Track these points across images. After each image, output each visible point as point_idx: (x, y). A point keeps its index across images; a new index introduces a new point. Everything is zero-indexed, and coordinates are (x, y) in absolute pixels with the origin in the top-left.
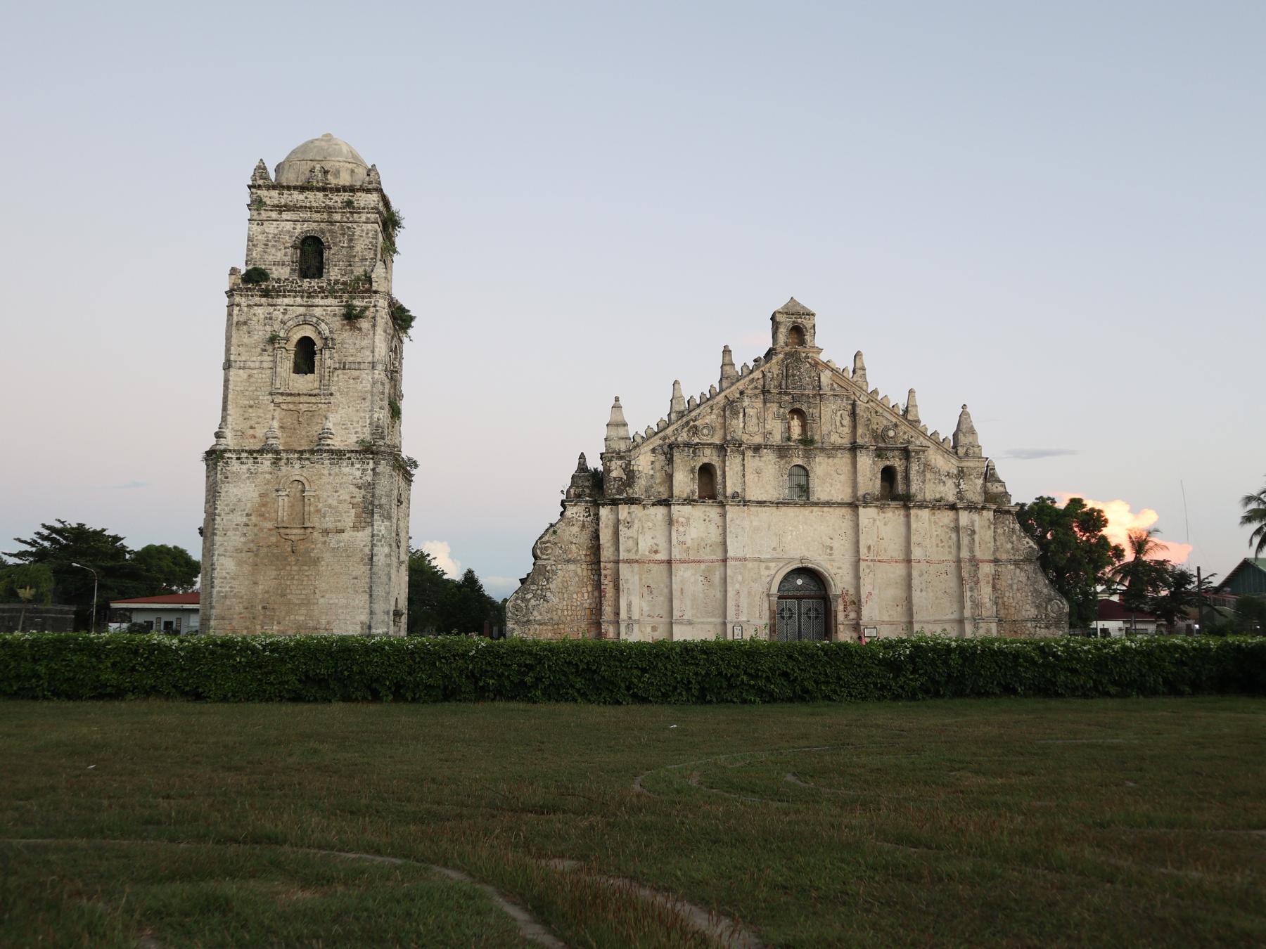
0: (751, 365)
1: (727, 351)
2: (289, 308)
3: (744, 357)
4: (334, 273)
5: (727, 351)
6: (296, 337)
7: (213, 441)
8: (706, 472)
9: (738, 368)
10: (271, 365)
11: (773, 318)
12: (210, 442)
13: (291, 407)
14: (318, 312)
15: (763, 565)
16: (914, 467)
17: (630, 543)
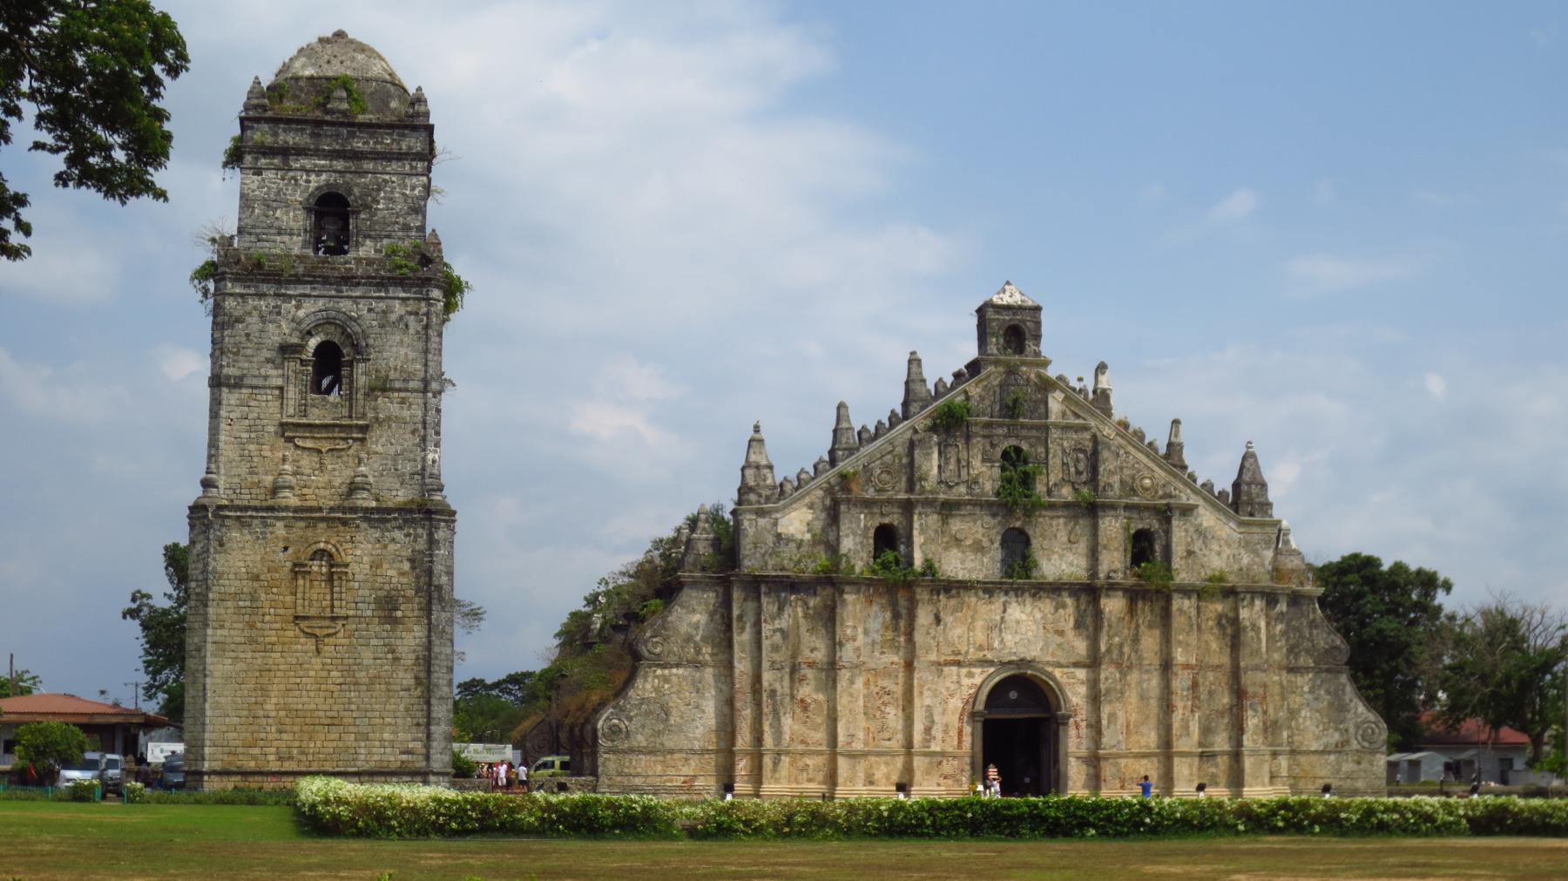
0: (949, 380)
1: (914, 361)
4: (367, 249)
5: (914, 361)
6: (313, 343)
7: (199, 491)
8: (886, 538)
9: (931, 386)
10: (279, 382)
11: (981, 311)
12: (194, 493)
13: (309, 444)
14: (345, 305)
15: (964, 671)
16: (1180, 533)
17: (778, 638)
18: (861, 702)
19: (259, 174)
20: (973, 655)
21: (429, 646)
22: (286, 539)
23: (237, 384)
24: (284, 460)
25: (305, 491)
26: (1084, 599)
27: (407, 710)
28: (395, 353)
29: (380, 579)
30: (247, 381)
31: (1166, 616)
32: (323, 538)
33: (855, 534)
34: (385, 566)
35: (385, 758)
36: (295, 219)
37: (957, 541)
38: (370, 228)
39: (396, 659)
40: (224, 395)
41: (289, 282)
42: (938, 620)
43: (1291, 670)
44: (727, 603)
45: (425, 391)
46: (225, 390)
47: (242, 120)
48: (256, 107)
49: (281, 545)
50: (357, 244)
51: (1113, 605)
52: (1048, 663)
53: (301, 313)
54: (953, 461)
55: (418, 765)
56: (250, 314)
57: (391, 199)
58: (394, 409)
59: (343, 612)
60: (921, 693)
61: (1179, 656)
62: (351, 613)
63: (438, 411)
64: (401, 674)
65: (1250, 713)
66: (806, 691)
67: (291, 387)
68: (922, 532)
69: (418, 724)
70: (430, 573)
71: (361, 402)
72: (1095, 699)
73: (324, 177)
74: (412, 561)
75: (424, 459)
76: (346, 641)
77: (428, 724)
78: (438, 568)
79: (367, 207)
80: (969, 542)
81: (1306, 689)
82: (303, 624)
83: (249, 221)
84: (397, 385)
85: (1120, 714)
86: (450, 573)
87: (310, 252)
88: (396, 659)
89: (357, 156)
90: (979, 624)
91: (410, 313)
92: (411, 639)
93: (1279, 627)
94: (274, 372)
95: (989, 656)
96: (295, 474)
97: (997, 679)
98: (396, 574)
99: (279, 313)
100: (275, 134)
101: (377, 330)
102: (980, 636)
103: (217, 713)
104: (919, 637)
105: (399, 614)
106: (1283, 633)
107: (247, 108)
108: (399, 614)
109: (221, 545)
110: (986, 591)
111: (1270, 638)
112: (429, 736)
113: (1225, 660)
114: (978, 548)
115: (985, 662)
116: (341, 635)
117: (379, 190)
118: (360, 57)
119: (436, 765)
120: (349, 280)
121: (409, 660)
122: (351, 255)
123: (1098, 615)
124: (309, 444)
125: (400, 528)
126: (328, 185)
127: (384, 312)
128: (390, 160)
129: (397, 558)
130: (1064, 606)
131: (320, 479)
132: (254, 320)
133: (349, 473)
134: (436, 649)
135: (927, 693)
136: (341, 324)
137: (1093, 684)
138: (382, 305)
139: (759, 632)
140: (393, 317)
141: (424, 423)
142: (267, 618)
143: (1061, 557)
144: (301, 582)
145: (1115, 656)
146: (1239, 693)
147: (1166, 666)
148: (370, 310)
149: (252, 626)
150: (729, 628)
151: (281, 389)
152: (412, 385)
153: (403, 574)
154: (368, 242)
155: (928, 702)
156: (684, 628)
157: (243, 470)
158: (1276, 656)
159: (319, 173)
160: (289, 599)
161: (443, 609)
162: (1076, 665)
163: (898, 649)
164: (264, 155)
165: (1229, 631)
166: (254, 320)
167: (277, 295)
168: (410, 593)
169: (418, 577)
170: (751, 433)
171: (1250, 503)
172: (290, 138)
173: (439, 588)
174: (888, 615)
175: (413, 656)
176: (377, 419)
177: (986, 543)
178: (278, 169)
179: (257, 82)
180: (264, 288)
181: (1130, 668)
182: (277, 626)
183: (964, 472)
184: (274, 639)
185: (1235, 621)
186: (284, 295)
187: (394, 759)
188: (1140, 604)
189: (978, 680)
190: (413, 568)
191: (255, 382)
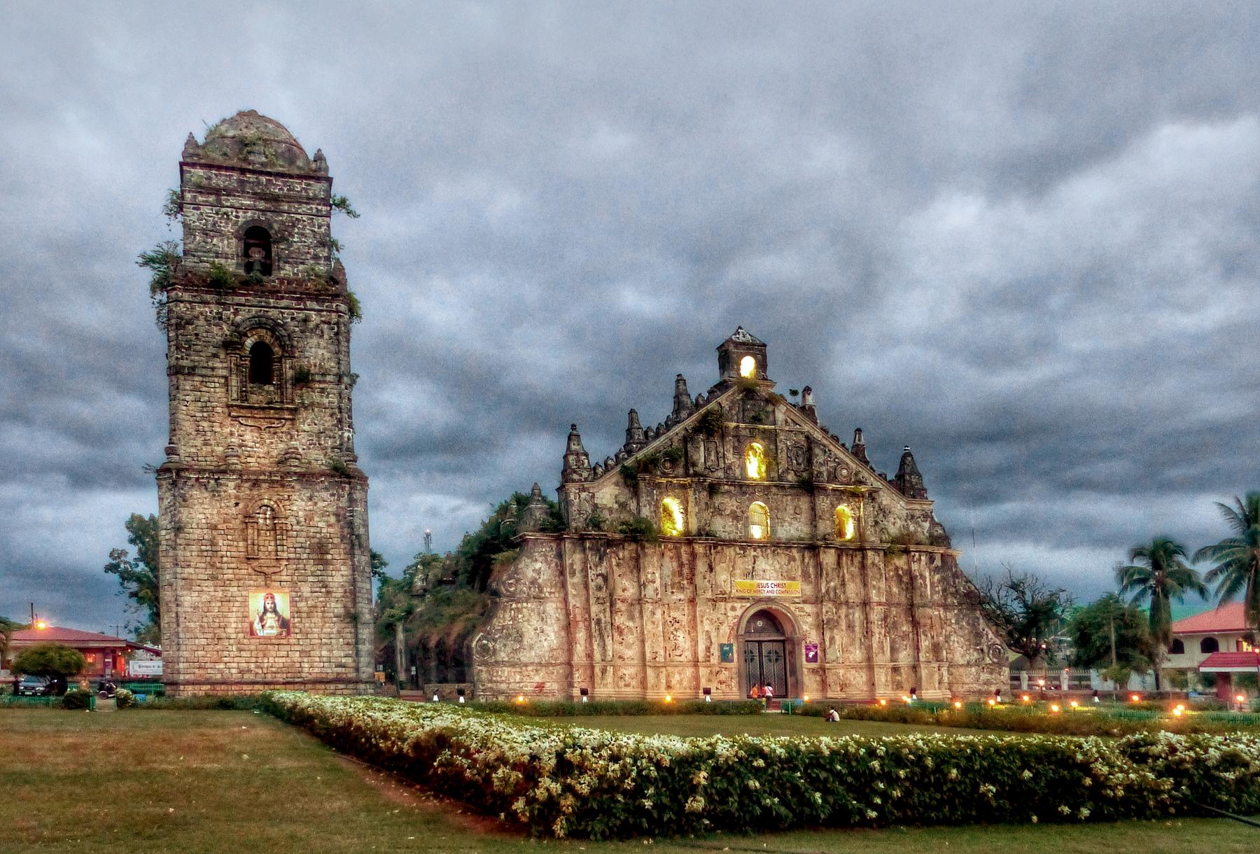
2: (244, 311)
6: (249, 342)
10: (225, 373)
14: (273, 313)
15: (729, 605)
18: (661, 628)
19: (198, 209)
20: (735, 593)
21: (354, 582)
22: (237, 497)
23: (192, 371)
24: (232, 434)
25: (249, 460)
26: (807, 554)
27: (339, 632)
28: (316, 352)
29: (312, 530)
30: (197, 371)
31: (863, 566)
32: (267, 496)
33: (650, 504)
34: (316, 519)
35: (324, 670)
37: (719, 511)
38: (288, 256)
39: (328, 593)
40: (181, 382)
41: (227, 294)
42: (711, 569)
43: (946, 607)
44: (560, 556)
45: (340, 382)
46: (182, 377)
47: (182, 164)
48: (192, 155)
49: (233, 501)
50: (280, 268)
52: (785, 599)
53: (238, 318)
54: (713, 453)
55: (350, 676)
56: (197, 318)
57: (303, 234)
58: (316, 397)
59: (285, 555)
61: (874, 596)
62: (292, 556)
63: (349, 400)
64: (333, 605)
66: (620, 620)
67: (234, 377)
69: (348, 644)
70: (351, 524)
71: (290, 391)
72: (821, 626)
73: (249, 214)
74: (337, 515)
75: (341, 437)
76: (288, 578)
77: (357, 643)
78: (357, 521)
79: (284, 239)
80: (728, 512)
82: (255, 563)
83: (192, 246)
84: (317, 378)
85: (837, 637)
86: (366, 526)
87: (241, 272)
88: (328, 593)
89: (276, 199)
91: (324, 322)
92: (339, 576)
94: (219, 365)
95: (746, 595)
96: (241, 446)
97: (752, 611)
98: (326, 527)
99: (220, 319)
100: (209, 178)
101: (299, 334)
103: (188, 635)
104: (698, 580)
105: (329, 557)
106: (939, 581)
107: (184, 155)
108: (329, 557)
109: (185, 501)
110: (742, 548)
111: (932, 584)
112: (357, 654)
113: (903, 600)
116: (284, 573)
117: (294, 226)
118: (271, 126)
119: (364, 676)
120: (274, 293)
121: (338, 593)
122: (275, 273)
123: (819, 566)
124: (250, 422)
125: (326, 489)
126: (253, 220)
127: (306, 320)
128: (300, 203)
129: (324, 514)
130: (794, 560)
131: (261, 451)
132: (201, 322)
133: (281, 446)
134: (359, 585)
135: (706, 622)
136: (274, 327)
137: (818, 615)
139: (586, 576)
140: (311, 325)
141: (340, 408)
142: (225, 559)
143: (790, 524)
144: (250, 531)
145: (832, 594)
146: (915, 624)
147: (865, 604)
148: (293, 319)
149: (213, 566)
150: (562, 573)
151: (226, 378)
152: (328, 378)
153: (330, 526)
154: (287, 267)
155: (707, 628)
157: (199, 442)
158: (936, 597)
159: (247, 209)
160: (241, 544)
162: (805, 602)
163: (683, 588)
164: (201, 193)
165: (905, 579)
166: (201, 322)
168: (336, 541)
169: (342, 528)
171: (912, 487)
173: (358, 537)
174: (675, 564)
175: (341, 590)
176: (303, 403)
179: (191, 136)
180: (208, 297)
181: (841, 604)
182: (233, 566)
183: (721, 461)
184: (231, 576)
185: (909, 572)
186: (224, 304)
187: (332, 671)
189: (739, 613)
190: (338, 521)
191: (204, 372)
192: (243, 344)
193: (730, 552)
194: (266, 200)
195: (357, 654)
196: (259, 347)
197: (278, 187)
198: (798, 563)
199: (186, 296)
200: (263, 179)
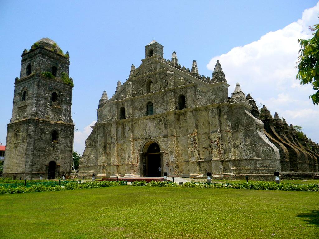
3: (137, 67)
6: (23, 92)
13: (21, 111)
36: (25, 71)
51: (171, 118)
60: (127, 149)
65: (213, 147)
68: (127, 107)
81: (242, 137)
90: (141, 129)
93: (225, 117)
102: (141, 132)
114: (141, 109)
115: (142, 139)
125: (26, 124)
126: (29, 64)
130: (161, 121)
138: (29, 82)
156: (92, 139)
161: (31, 139)
162: (164, 137)
166: (17, 90)
167: (20, 85)
170: (103, 93)
172: (26, 57)
173: (30, 135)
177: (143, 107)
178: (24, 63)
180: (19, 84)
188: (181, 117)
191: (16, 101)
192: (21, 94)
193: (138, 122)
194: (32, 58)
195: (26, 166)
196: (25, 92)
197: (33, 54)
198: (163, 122)
199: (16, 85)
200: (31, 53)
